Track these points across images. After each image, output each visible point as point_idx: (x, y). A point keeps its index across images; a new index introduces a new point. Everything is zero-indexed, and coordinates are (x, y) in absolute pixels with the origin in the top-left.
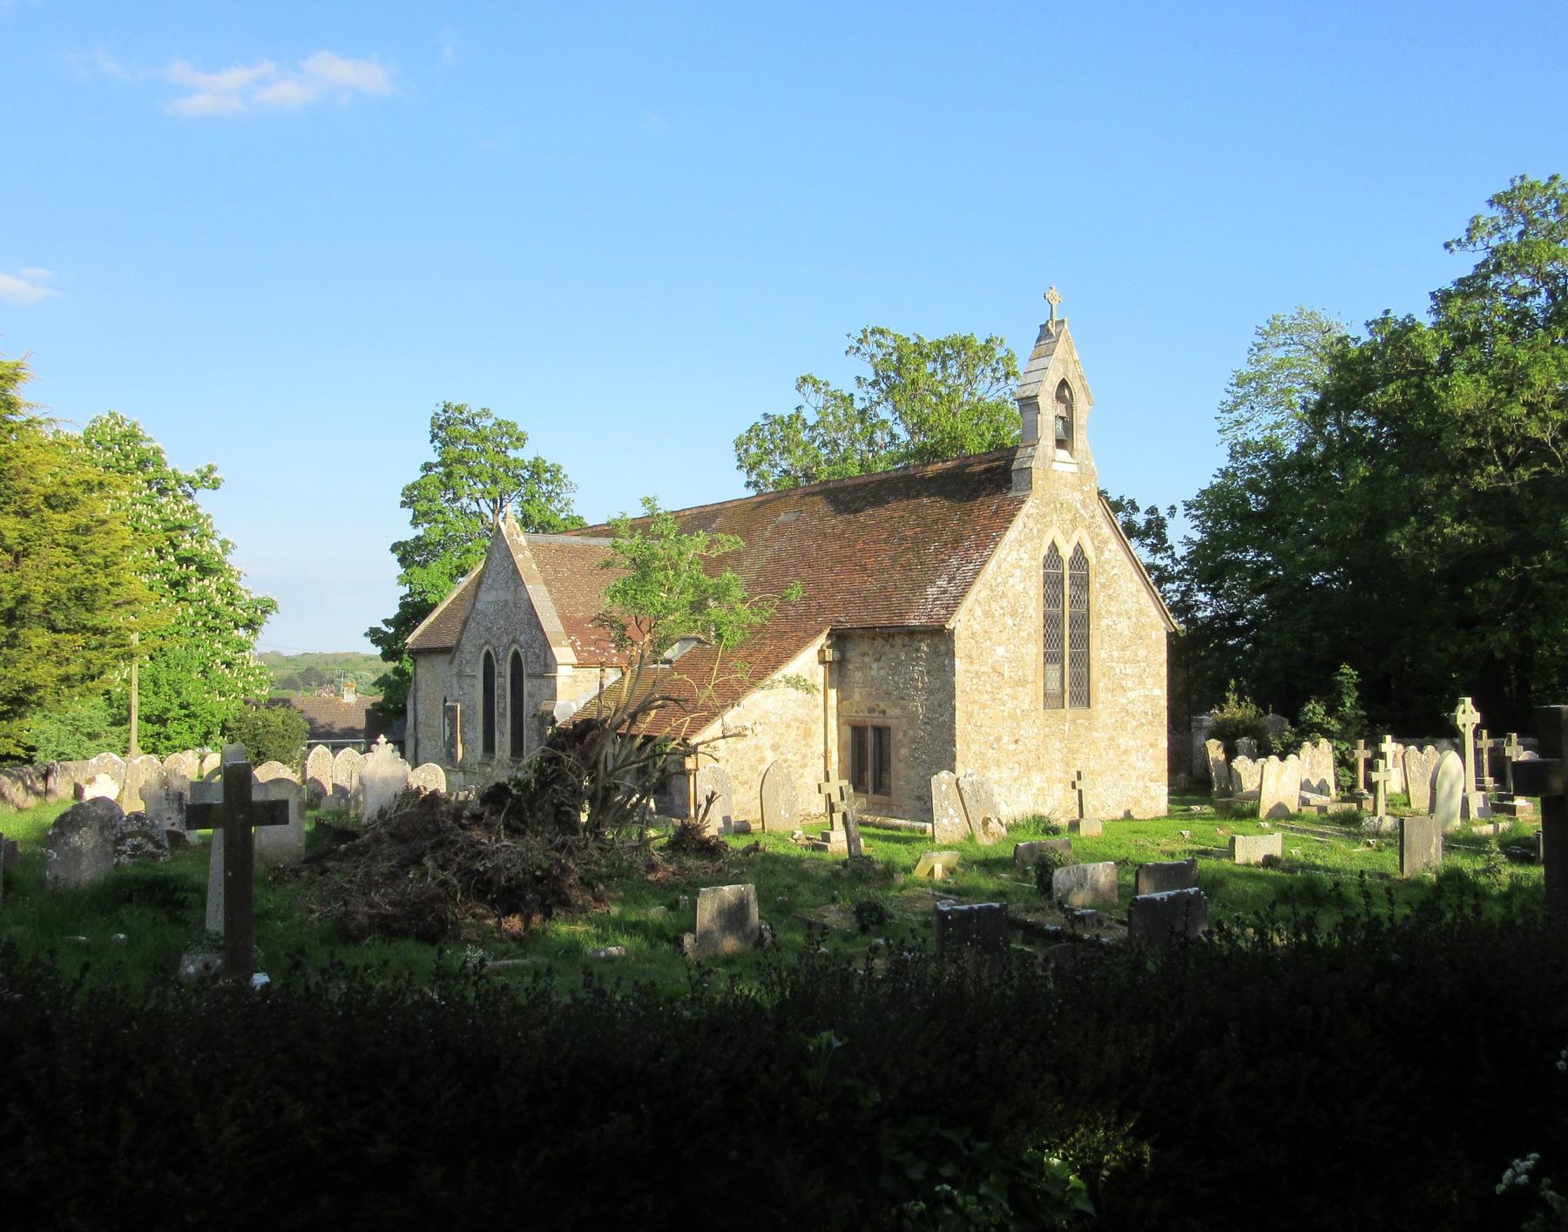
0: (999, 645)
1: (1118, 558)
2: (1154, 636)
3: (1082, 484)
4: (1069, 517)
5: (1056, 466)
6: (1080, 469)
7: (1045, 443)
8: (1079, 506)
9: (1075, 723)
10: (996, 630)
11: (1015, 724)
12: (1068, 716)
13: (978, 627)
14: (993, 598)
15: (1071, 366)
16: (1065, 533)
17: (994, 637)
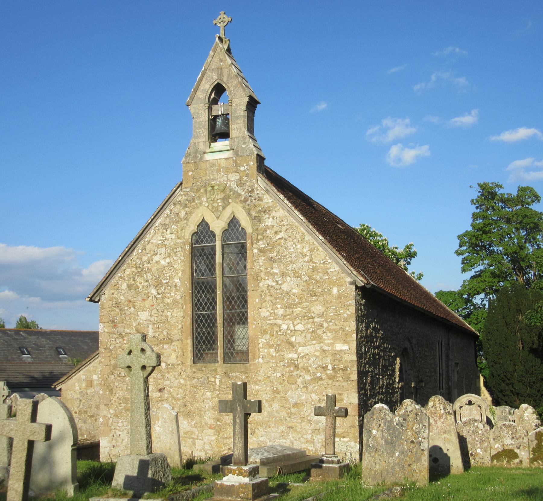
0: (144, 310)
2: (335, 291)
3: (237, 165)
4: (221, 196)
5: (208, 157)
7: (197, 140)
8: (234, 185)
9: (229, 377)
10: (139, 298)
11: (159, 375)
13: (122, 298)
14: (140, 274)
15: (225, 71)
16: (214, 210)
17: (138, 304)
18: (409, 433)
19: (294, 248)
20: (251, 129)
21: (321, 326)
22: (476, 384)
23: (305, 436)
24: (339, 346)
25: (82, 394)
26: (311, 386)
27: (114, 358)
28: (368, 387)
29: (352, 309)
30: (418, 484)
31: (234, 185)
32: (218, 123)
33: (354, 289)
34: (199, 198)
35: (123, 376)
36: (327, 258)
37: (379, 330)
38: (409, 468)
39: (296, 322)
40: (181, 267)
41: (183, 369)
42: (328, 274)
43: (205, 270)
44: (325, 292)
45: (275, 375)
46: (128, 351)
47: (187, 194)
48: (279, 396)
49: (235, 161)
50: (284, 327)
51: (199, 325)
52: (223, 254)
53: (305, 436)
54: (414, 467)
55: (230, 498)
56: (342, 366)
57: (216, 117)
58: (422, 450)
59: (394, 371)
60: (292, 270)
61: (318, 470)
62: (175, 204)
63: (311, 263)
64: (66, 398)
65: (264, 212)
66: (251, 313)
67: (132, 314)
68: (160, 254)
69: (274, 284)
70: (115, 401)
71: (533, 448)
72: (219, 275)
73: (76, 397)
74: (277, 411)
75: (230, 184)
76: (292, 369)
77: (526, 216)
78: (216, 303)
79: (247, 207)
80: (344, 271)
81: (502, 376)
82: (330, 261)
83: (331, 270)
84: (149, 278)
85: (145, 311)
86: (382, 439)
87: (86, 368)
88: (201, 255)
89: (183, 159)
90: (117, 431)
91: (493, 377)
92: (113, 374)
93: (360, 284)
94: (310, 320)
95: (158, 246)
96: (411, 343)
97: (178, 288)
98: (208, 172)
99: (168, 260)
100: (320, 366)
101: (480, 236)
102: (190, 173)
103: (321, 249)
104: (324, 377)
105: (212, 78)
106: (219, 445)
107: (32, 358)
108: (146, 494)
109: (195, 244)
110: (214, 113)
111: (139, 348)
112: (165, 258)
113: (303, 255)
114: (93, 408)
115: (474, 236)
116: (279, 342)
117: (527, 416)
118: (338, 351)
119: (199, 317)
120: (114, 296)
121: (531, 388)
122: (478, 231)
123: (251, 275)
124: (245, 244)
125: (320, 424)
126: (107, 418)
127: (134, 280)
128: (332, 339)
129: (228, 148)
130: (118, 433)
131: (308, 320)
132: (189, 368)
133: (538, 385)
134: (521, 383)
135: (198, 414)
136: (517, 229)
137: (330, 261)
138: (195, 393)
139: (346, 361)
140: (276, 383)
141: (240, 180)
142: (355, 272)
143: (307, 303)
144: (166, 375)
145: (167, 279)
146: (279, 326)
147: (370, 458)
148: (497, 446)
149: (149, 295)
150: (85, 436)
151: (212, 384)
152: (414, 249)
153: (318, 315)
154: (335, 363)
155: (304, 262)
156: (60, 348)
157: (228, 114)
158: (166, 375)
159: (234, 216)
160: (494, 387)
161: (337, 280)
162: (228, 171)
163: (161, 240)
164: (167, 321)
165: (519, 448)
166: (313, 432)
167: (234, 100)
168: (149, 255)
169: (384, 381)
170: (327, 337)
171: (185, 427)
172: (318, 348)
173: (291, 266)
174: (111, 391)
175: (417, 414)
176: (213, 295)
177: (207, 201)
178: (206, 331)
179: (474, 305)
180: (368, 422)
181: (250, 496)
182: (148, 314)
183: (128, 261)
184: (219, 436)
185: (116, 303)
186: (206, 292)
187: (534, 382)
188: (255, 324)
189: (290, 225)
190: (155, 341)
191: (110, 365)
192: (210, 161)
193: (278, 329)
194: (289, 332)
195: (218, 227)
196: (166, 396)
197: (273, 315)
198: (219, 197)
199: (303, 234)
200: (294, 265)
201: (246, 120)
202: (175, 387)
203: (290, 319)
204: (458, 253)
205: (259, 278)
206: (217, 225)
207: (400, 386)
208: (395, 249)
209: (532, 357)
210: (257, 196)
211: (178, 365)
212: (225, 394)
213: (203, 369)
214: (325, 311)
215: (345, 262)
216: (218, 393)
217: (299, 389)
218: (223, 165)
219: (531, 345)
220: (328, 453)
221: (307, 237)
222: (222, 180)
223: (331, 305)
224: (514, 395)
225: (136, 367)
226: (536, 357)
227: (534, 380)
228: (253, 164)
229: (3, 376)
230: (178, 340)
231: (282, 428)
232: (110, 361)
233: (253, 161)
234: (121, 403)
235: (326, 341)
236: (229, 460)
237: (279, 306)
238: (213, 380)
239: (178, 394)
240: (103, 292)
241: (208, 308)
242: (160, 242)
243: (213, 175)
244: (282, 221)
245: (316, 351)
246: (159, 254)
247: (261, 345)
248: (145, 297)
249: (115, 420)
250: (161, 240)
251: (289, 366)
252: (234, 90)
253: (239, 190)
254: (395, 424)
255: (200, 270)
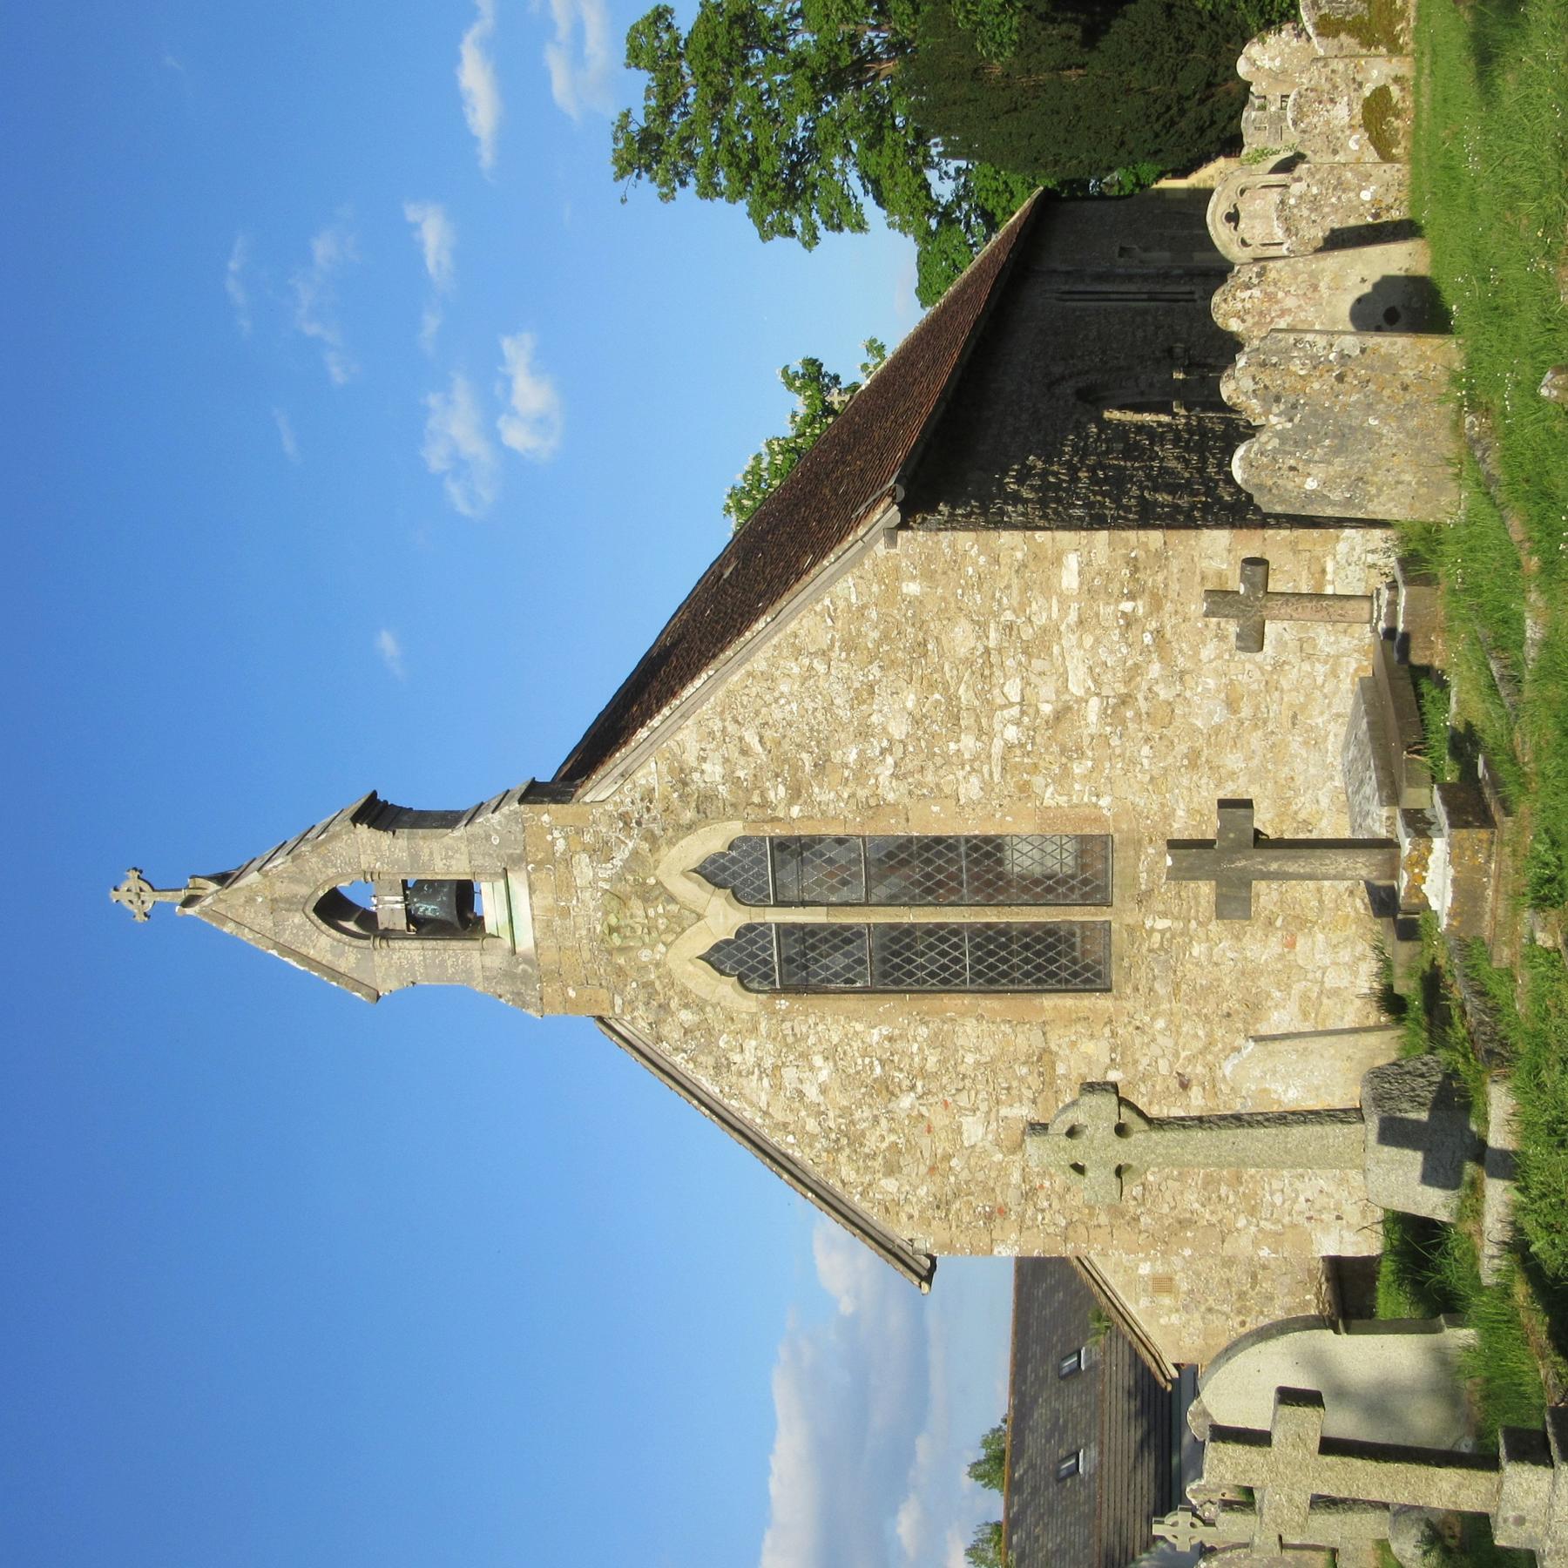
0: (959, 1130)
1: (716, 725)
2: (912, 588)
3: (549, 860)
4: (636, 906)
5: (525, 942)
6: (519, 860)
7: (478, 974)
8: (606, 871)
10: (925, 1142)
12: (1129, 920)
13: (922, 1191)
14: (856, 1140)
15: (282, 889)
17: (942, 1147)
18: (1316, 386)
19: (789, 703)
20: (448, 820)
21: (1011, 629)
22: (1181, 201)
23: (1320, 680)
24: (1069, 578)
25: (1193, 1305)
26: (1180, 660)
27: (1091, 1215)
28: (1184, 502)
29: (966, 540)
30: (1457, 366)
31: (606, 871)
32: (429, 913)
33: (910, 533)
34: (642, 968)
35: (1144, 1189)
36: (818, 608)
37: (1024, 465)
38: (1412, 388)
39: (1000, 701)
40: (838, 1022)
41: (1126, 1020)
42: (864, 607)
43: (846, 955)
44: (914, 615)
45: (1145, 762)
46: (1074, 1175)
47: (630, 1004)
48: (1206, 752)
49: (540, 865)
50: (1012, 733)
51: (1004, 974)
52: (804, 904)
53: (1320, 680)
54: (1409, 375)
55: (1489, 892)
56: (1126, 572)
57: (412, 918)
58: (1363, 351)
59: (1141, 428)
60: (852, 708)
61: (1413, 644)
62: (659, 1039)
63: (834, 655)
64: (1201, 1351)
65: (685, 784)
66: (971, 826)
67: (968, 1163)
68: (801, 1081)
69: (890, 760)
70: (1212, 1213)
71: (1362, 44)
72: (860, 915)
73: (1199, 1323)
74: (1248, 759)
75: (605, 880)
76: (1130, 714)
77: (710, 47)
78: (941, 926)
79: (670, 832)
80: (857, 561)
81: (1157, 127)
82: (827, 602)
83: (853, 599)
84: (867, 1113)
85: (960, 1127)
86: (1330, 463)
87: (1120, 1294)
88: (805, 967)
89: (531, 1012)
90: (1297, 1207)
91: (1160, 150)
92: (1136, 1219)
93: (894, 515)
94: (994, 659)
95: (777, 1087)
96: (1063, 378)
97: (897, 1032)
98: (568, 944)
99: (818, 1061)
100: (1122, 635)
101: (765, 179)
102: (572, 993)
103: (793, 625)
104: (1154, 625)
105: (300, 927)
106: (1341, 922)
107: (1086, 1445)
108: (1474, 1127)
109: (774, 982)
110: (401, 923)
111: (1065, 1142)
112: (812, 1068)
113: (810, 677)
114: (1230, 1275)
115: (764, 194)
116: (1055, 749)
117: (1272, 59)
118: (1081, 584)
119: (980, 974)
120: (916, 1214)
121: (1193, 47)
122: (749, 184)
123: (862, 824)
124: (776, 841)
125: (1287, 637)
126: (1260, 1236)
127: (874, 1156)
128: (1048, 599)
129: (502, 882)
130: (1301, 1204)
131: (992, 666)
132: (1124, 1004)
133: (1184, 27)
134: (1179, 76)
135: (1253, 981)
136: (747, 73)
137: (827, 602)
138: (1194, 989)
139: (1111, 560)
140: (1170, 760)
141: (592, 852)
142: (861, 531)
143: (947, 668)
144: (1141, 1068)
145: (872, 1062)
146: (1009, 747)
147: (1383, 498)
148: (1353, 146)
149: (915, 1113)
150: (1308, 1297)
151: (1170, 941)
152: (797, 366)
153: (979, 638)
154: (1116, 592)
155: (828, 673)
156: (1060, 1368)
157: (404, 882)
158: (1141, 1068)
159: (695, 871)
160: (1188, 151)
161: (881, 581)
162: (565, 886)
163: (761, 1079)
164: (990, 1066)
165: (1360, 85)
166: (1309, 656)
167: (364, 867)
168: (803, 1113)
169: (1169, 456)
170: (1043, 612)
171: (1287, 1018)
172: (1074, 638)
173: (841, 713)
174: (1184, 1224)
175: (1263, 364)
176: (918, 934)
177: (653, 947)
178: (1019, 954)
179: (959, 199)
180: (1282, 501)
181: (1483, 834)
182: (970, 1119)
183: (817, 1172)
184: (1316, 923)
185: (938, 1207)
186: (908, 954)
187: (1178, 39)
188: (1004, 816)
189: (722, 712)
190: (1046, 1100)
191: (1112, 1226)
192: (538, 935)
193: (1018, 752)
194: (1026, 719)
195: (725, 917)
196: (1199, 1069)
197: (977, 765)
198: (641, 913)
199: (749, 674)
200: (838, 701)
201: (420, 831)
202: (1176, 1044)
203: (990, 718)
204: (811, 241)
205: (873, 802)
206: (721, 919)
207: (1183, 412)
208: (798, 419)
209: (1105, 43)
210: (640, 805)
211: (1114, 1034)
212: (1198, 904)
213: (1126, 964)
214: (969, 616)
215: (832, 557)
216: (1193, 924)
217: (1188, 694)
218: (550, 901)
219: (1072, 43)
220: (1366, 617)
221: (759, 663)
222: (592, 904)
223: (952, 600)
224: (1213, 95)
225: (1120, 1151)
226: (1106, 32)
227: (1171, 39)
228: (546, 814)
229: (1138, 1526)
230: (1044, 1034)
231: (1295, 744)
232: (1099, 1226)
233: (539, 815)
234: (1219, 1196)
235: (1055, 616)
236: (1383, 894)
237: (953, 746)
238: (1157, 937)
239: (1196, 1036)
240: (904, 1245)
241: (956, 947)
242: (766, 1081)
243: (576, 928)
244: (711, 733)
245: (1080, 646)
246: (800, 1086)
247: (1062, 800)
248: (923, 1125)
249: (1265, 1213)
250: (761, 1079)
251: (1123, 722)
252: (335, 866)
253: (620, 856)
254: (1289, 425)
255: (848, 968)
